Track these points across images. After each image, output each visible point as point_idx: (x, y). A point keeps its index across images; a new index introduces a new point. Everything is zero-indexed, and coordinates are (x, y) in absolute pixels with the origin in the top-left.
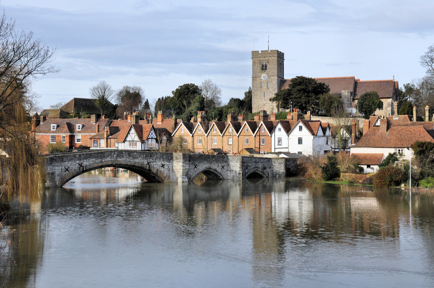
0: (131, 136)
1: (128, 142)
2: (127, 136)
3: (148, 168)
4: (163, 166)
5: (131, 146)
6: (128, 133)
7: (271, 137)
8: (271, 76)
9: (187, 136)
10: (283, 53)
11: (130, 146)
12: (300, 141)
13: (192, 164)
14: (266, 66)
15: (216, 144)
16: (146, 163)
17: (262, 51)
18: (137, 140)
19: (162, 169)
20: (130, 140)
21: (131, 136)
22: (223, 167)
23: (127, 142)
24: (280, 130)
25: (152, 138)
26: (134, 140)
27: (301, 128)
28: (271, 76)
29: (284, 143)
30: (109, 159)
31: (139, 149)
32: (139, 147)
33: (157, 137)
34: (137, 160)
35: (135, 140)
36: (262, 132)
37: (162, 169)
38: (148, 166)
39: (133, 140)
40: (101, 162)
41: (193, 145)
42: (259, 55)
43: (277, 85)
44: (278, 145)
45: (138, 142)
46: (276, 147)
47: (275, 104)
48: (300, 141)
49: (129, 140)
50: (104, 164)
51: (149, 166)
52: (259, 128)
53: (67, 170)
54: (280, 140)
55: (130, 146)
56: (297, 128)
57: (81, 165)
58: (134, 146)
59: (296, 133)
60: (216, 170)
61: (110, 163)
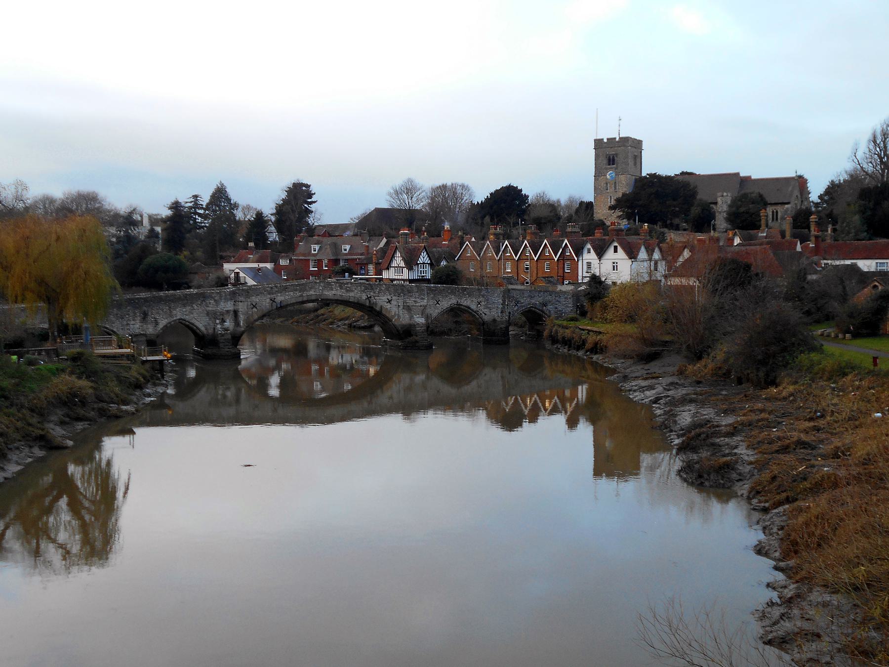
3: (367, 304)
4: (389, 301)
7: (578, 261)
10: (642, 141)
13: (433, 299)
14: (614, 160)
15: (510, 271)
16: (364, 297)
17: (608, 139)
19: (388, 306)
22: (479, 304)
24: (589, 252)
25: (424, 263)
27: (616, 251)
30: (312, 292)
32: (406, 274)
33: (431, 261)
34: (352, 294)
37: (388, 306)
38: (368, 301)
40: (301, 296)
42: (605, 145)
45: (404, 269)
46: (585, 274)
47: (618, 213)
50: (305, 299)
51: (370, 302)
53: (254, 306)
54: (589, 264)
57: (273, 300)
59: (610, 254)
60: (469, 308)
61: (313, 298)
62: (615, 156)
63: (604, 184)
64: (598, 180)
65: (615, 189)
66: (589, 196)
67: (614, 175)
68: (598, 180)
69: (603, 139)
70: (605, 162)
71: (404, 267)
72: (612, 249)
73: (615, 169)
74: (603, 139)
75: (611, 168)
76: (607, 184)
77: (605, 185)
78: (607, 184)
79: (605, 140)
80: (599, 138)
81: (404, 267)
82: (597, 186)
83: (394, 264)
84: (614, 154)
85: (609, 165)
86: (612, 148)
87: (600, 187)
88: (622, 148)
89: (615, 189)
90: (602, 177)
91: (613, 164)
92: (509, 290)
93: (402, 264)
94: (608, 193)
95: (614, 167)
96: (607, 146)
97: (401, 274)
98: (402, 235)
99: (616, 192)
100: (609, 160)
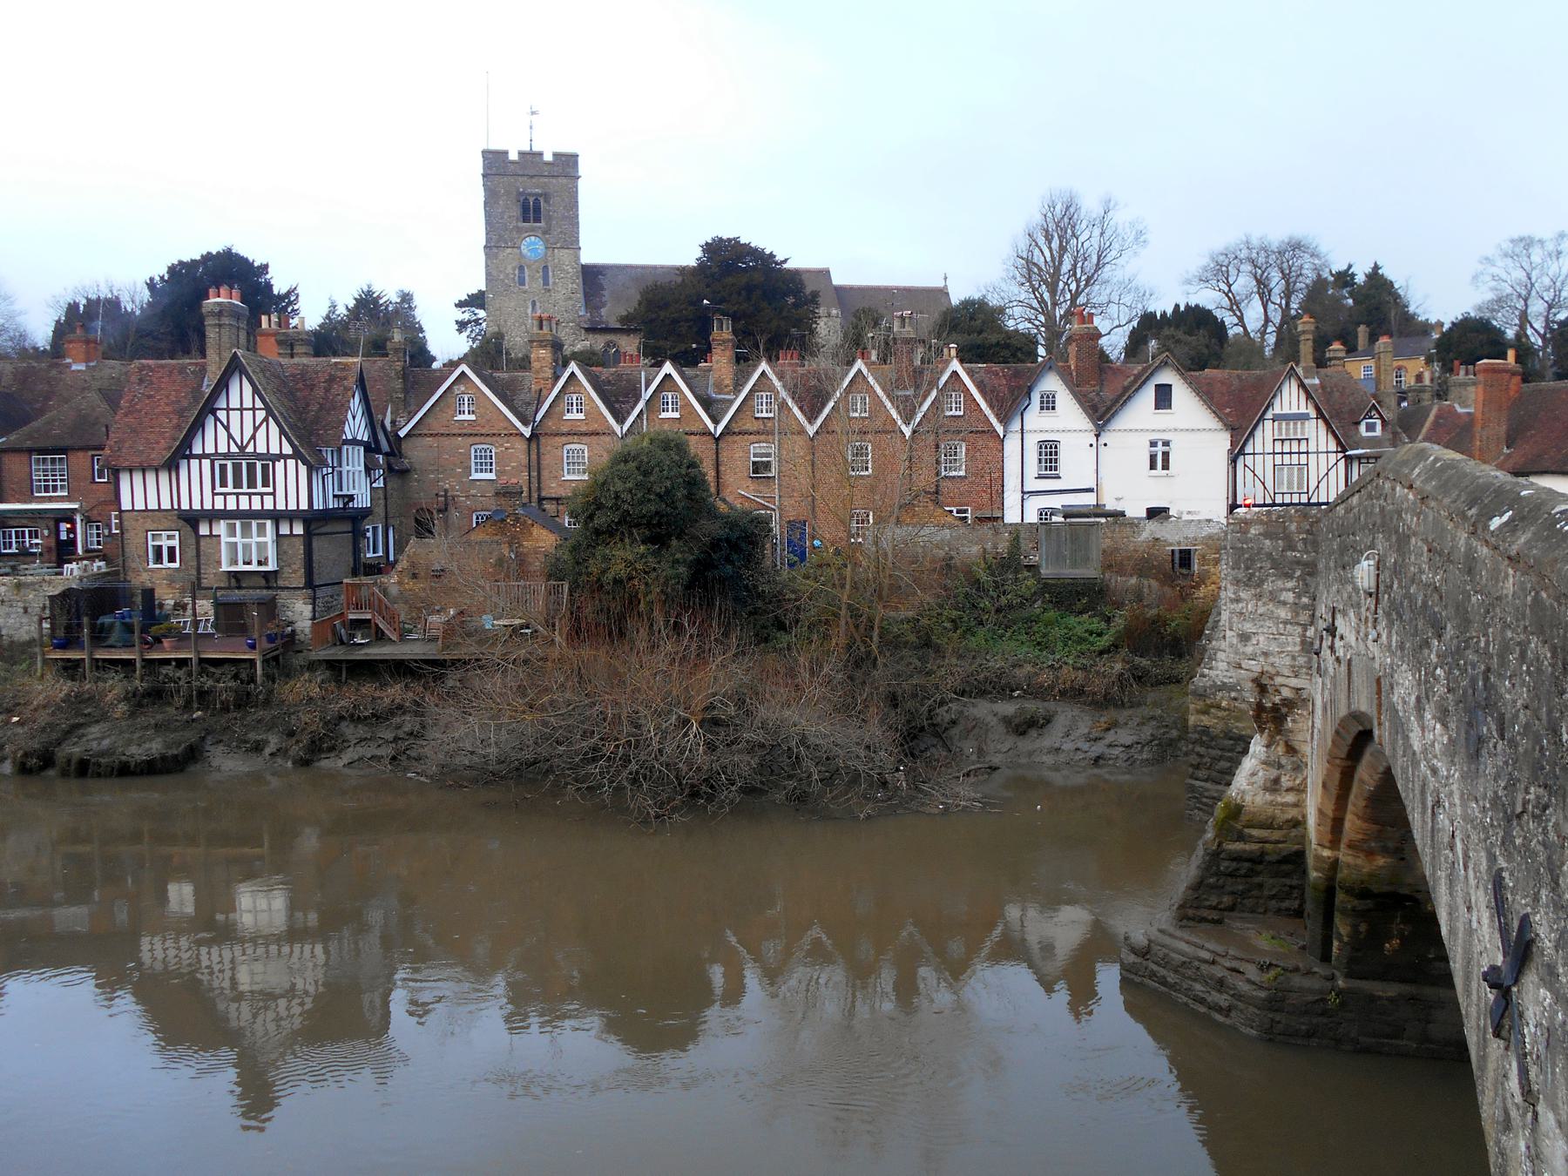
0: (227, 428)
1: (206, 463)
2: (198, 426)
5: (230, 489)
6: (209, 408)
8: (558, 245)
9: (495, 438)
11: (218, 489)
12: (1160, 460)
14: (537, 209)
17: (521, 154)
18: (275, 450)
20: (223, 449)
21: (227, 428)
23: (195, 463)
24: (1048, 404)
26: (250, 449)
27: (1163, 398)
28: (558, 245)
29: (1076, 466)
31: (292, 506)
35: (261, 449)
36: (949, 413)
39: (242, 448)
41: (534, 481)
43: (581, 279)
44: (1040, 477)
48: (1160, 460)
49: (210, 449)
52: (941, 391)
54: (1049, 454)
55: (224, 484)
56: (1148, 395)
58: (252, 484)
62: (542, 200)
63: (514, 269)
64: (496, 257)
65: (546, 282)
66: (484, 289)
67: (540, 247)
68: (496, 257)
69: (506, 153)
70: (516, 211)
71: (286, 457)
72: (1148, 395)
73: (545, 233)
74: (506, 153)
75: (533, 230)
76: (521, 268)
77: (517, 272)
78: (521, 268)
79: (513, 156)
80: (494, 146)
81: (281, 456)
82: (495, 273)
83: (212, 440)
84: (541, 195)
85: (526, 220)
86: (532, 177)
87: (502, 277)
88: (560, 180)
89: (546, 282)
90: (509, 250)
91: (538, 220)
92: (87, 551)
93: (271, 440)
94: (525, 292)
95: (540, 228)
96: (521, 173)
97: (260, 489)
98: (220, 314)
99: (549, 290)
100: (525, 208)
